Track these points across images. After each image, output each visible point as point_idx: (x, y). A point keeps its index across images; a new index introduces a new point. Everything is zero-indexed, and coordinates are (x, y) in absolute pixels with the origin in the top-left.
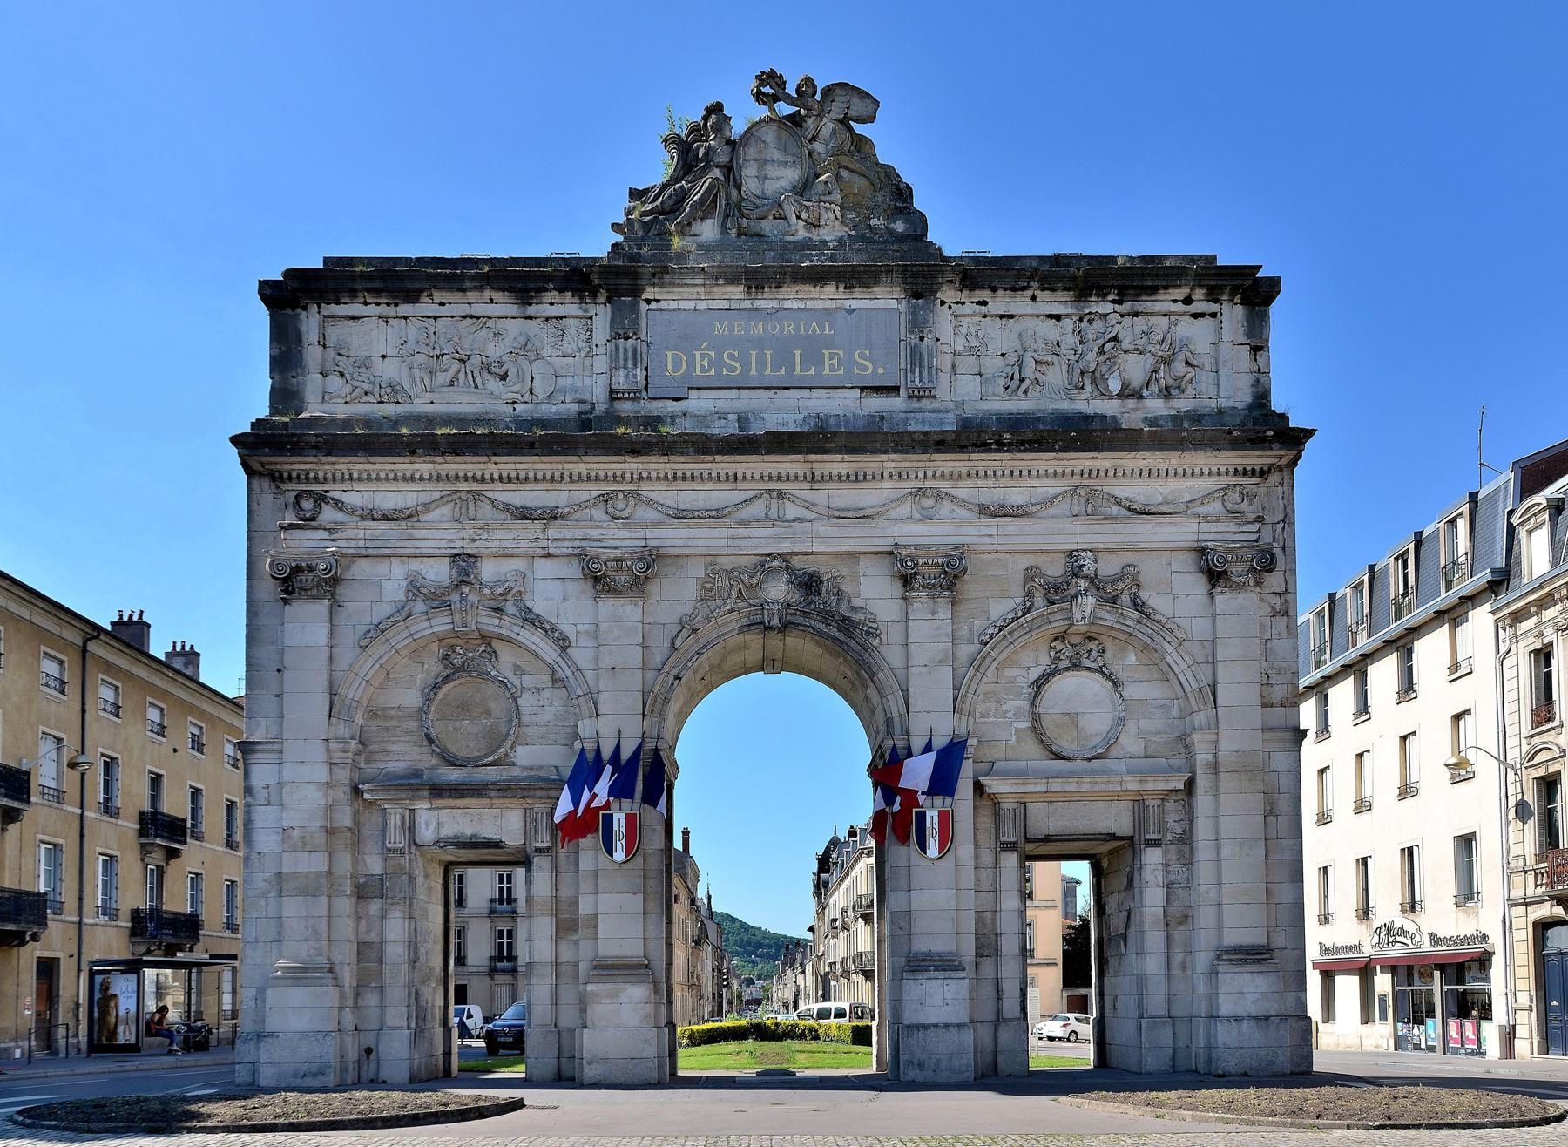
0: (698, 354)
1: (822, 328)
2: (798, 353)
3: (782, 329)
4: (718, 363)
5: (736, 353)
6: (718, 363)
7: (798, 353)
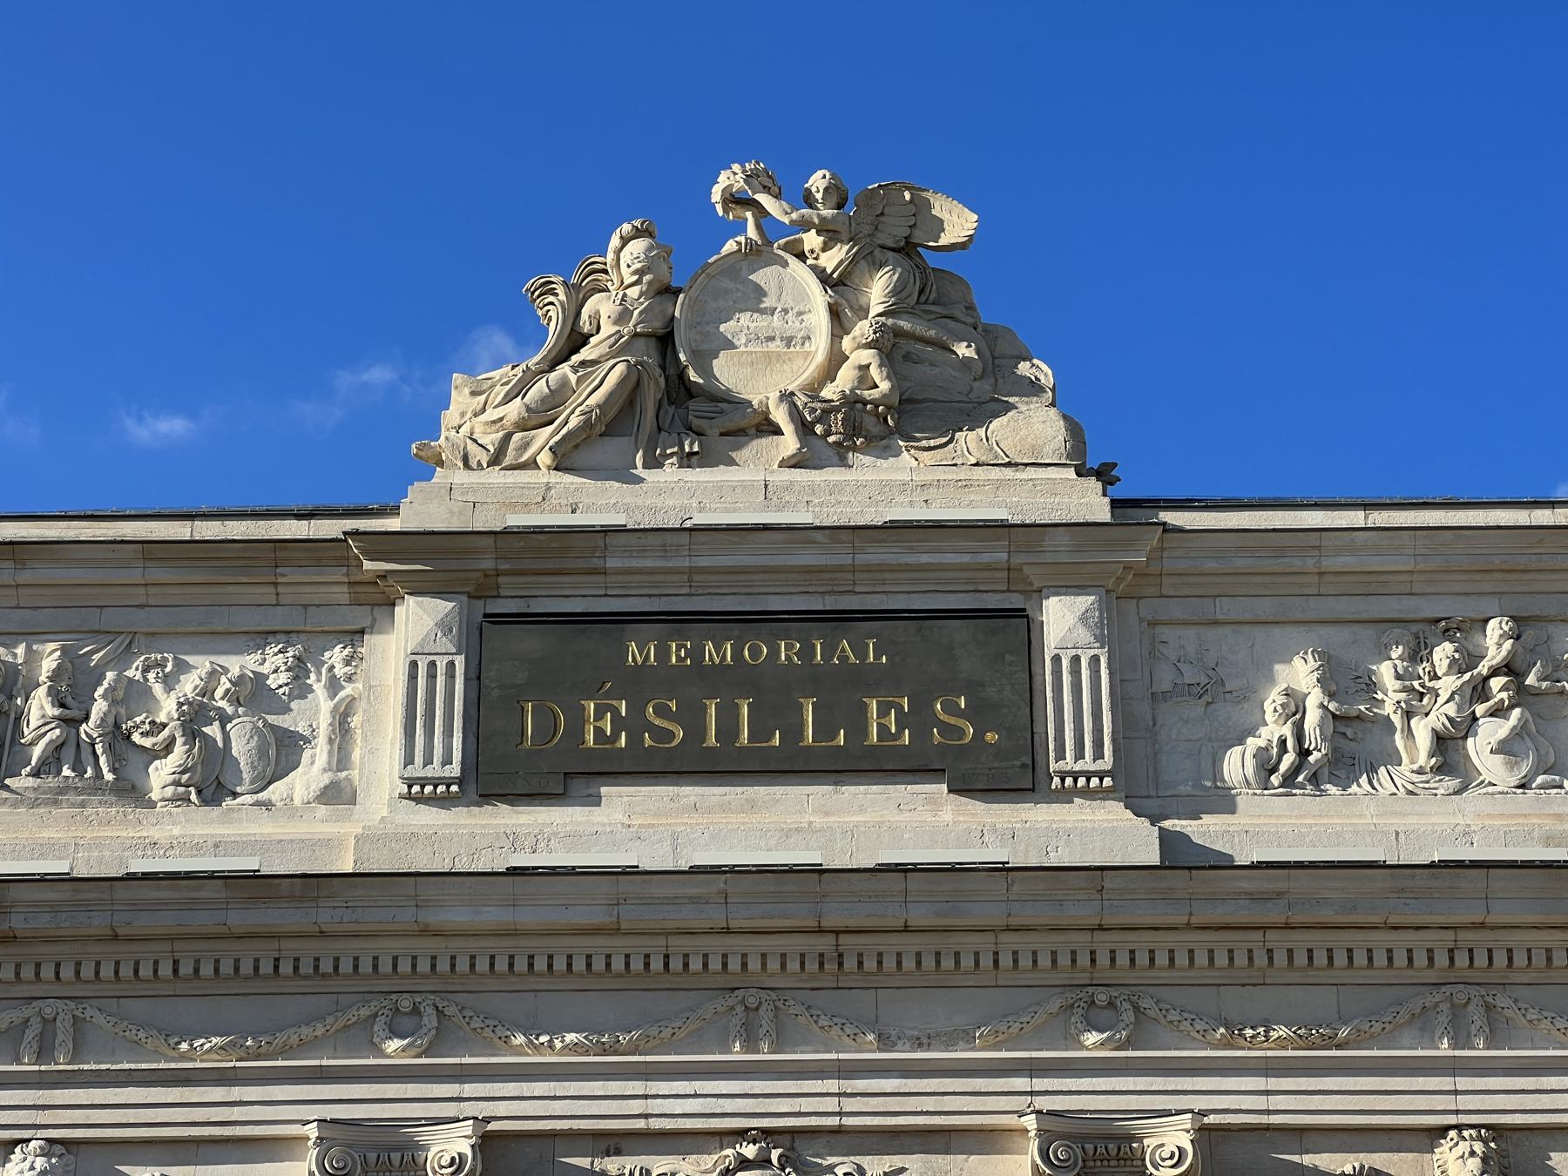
1: (861, 652)
3: (774, 652)
5: (673, 706)
6: (634, 725)
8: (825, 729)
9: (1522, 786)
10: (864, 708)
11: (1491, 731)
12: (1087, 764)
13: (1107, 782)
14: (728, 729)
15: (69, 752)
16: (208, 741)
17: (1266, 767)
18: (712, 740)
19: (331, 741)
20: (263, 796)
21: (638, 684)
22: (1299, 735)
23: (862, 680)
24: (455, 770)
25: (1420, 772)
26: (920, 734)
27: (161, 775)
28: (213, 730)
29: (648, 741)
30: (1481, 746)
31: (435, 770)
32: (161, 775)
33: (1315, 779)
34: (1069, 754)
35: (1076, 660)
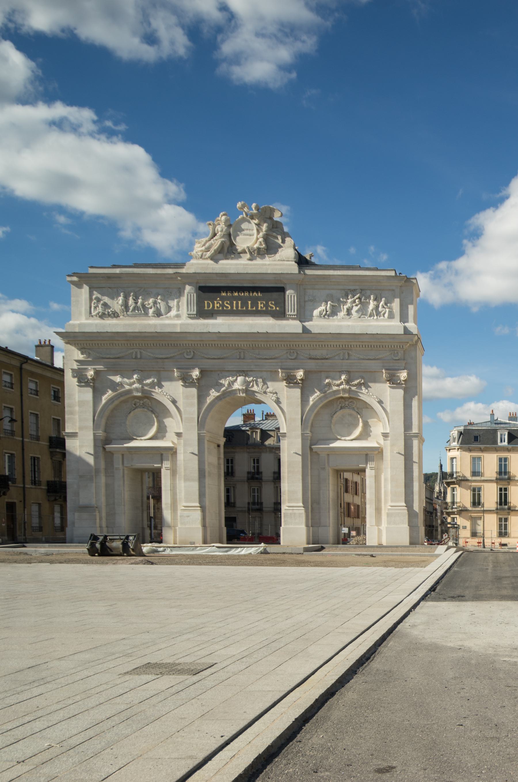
0: (215, 302)
2: (250, 302)
4: (223, 305)
6: (223, 305)
7: (250, 302)
8: (252, 307)
9: (359, 317)
10: (258, 303)
11: (355, 309)
12: (292, 313)
13: (295, 316)
14: (237, 306)
15: (136, 308)
16: (157, 307)
17: (321, 313)
18: (235, 308)
19: (177, 307)
20: (167, 316)
21: (223, 299)
22: (326, 309)
23: (258, 299)
24: (195, 313)
25: (344, 315)
26: (267, 308)
27: (151, 311)
28: (158, 306)
29: (225, 308)
30: (354, 311)
31: (192, 313)
32: (151, 311)
33: (328, 316)
34: (290, 311)
35: (291, 296)
